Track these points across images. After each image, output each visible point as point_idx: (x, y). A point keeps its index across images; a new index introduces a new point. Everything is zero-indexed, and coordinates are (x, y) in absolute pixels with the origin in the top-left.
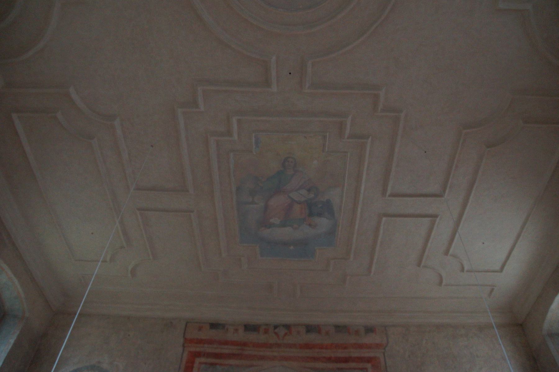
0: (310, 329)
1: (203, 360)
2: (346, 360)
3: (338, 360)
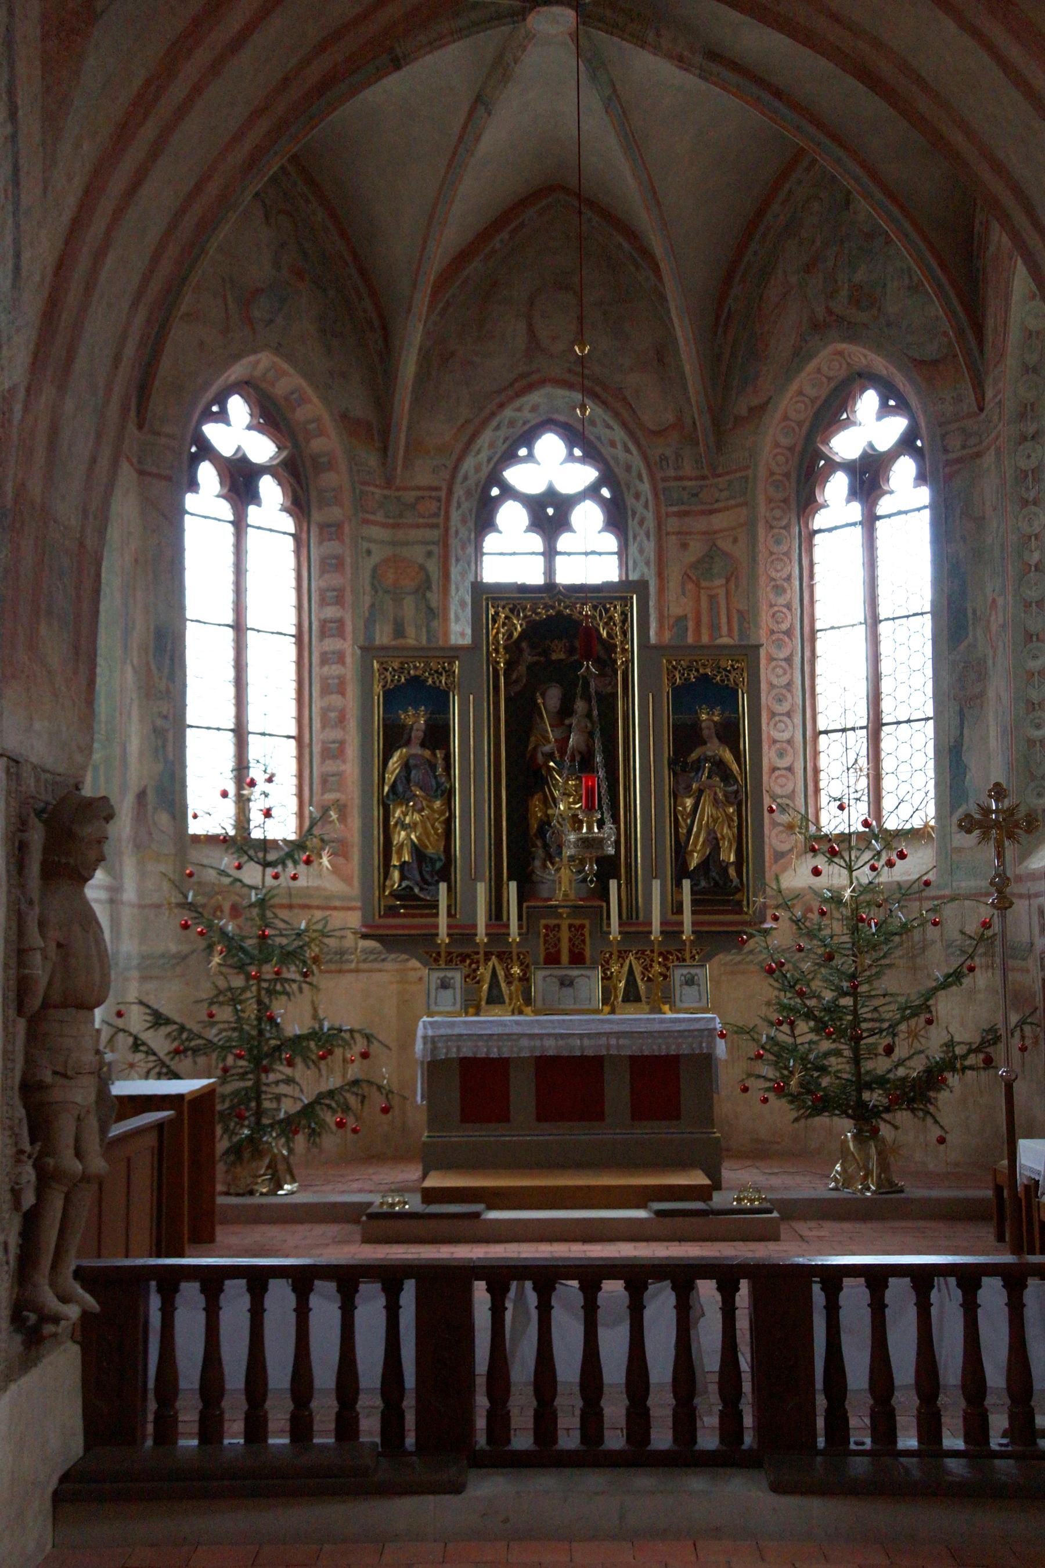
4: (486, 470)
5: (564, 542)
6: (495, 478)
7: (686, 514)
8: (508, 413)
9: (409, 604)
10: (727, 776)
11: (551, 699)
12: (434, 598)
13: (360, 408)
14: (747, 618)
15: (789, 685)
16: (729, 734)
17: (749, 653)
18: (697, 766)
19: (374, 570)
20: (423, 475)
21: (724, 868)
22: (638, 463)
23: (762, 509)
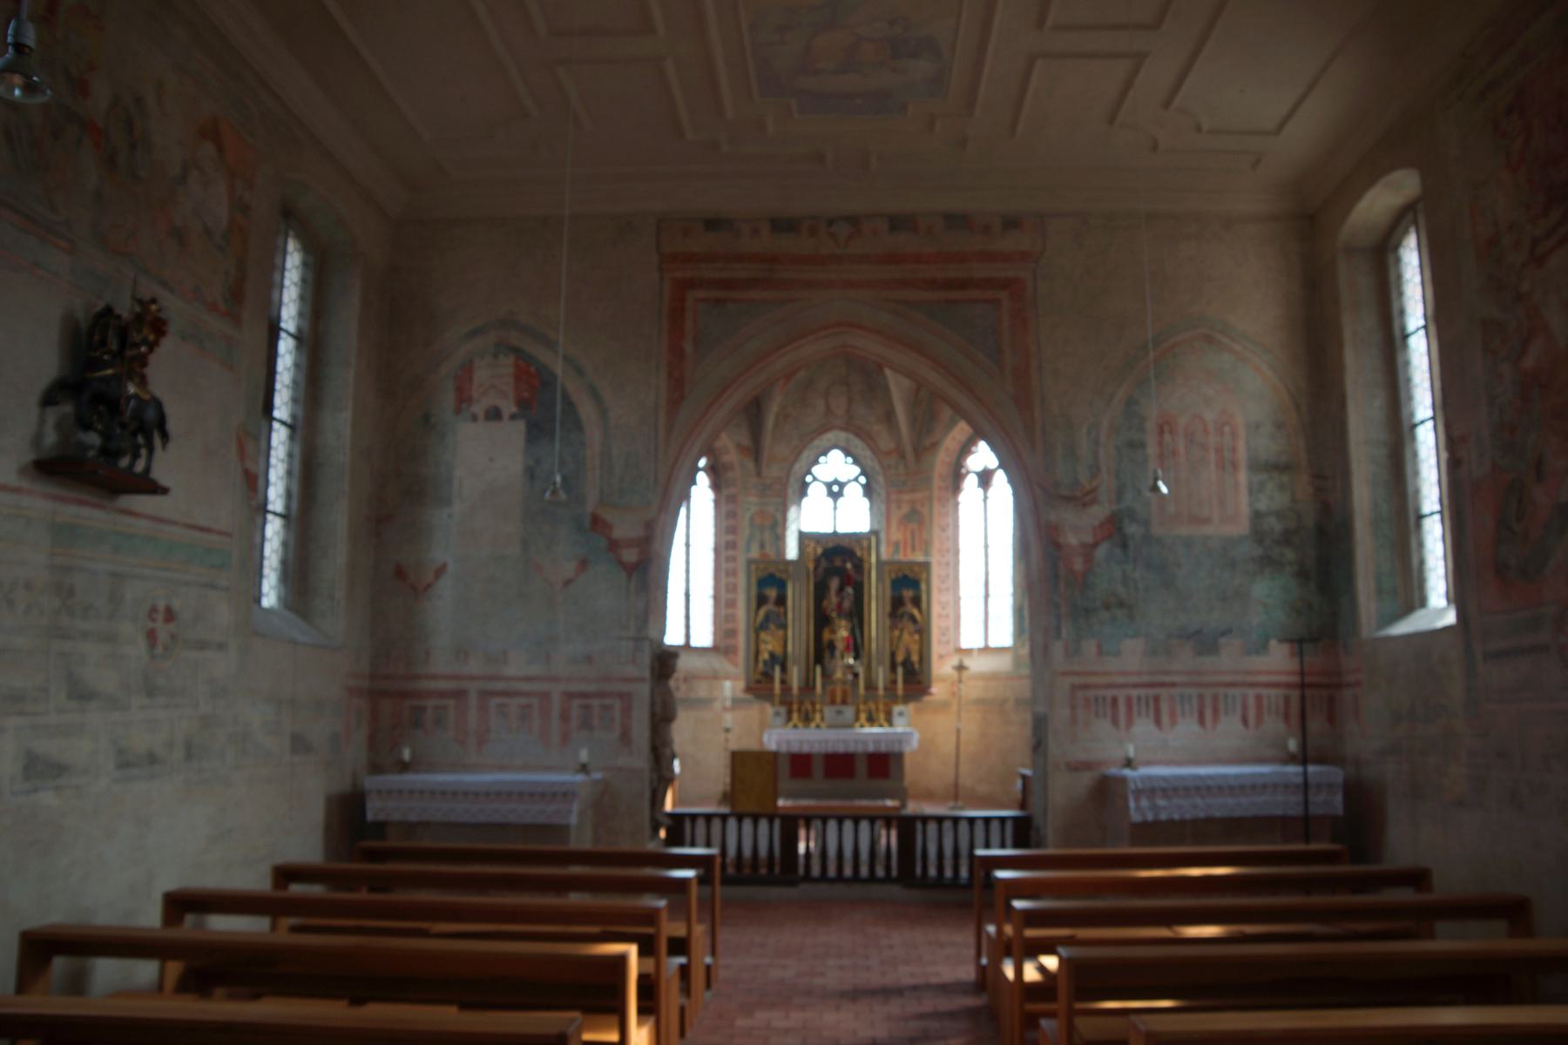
0: (897, 223)
1: (701, 294)
2: (963, 284)
3: (948, 285)
4: (805, 469)
5: (841, 500)
6: (809, 472)
7: (900, 492)
8: (817, 442)
9: (767, 535)
10: (913, 619)
11: (834, 583)
12: (779, 530)
13: (746, 441)
14: (927, 547)
15: (947, 576)
16: (917, 601)
17: (926, 566)
18: (902, 616)
19: (752, 520)
20: (773, 471)
21: (912, 665)
22: (877, 467)
23: (936, 493)
